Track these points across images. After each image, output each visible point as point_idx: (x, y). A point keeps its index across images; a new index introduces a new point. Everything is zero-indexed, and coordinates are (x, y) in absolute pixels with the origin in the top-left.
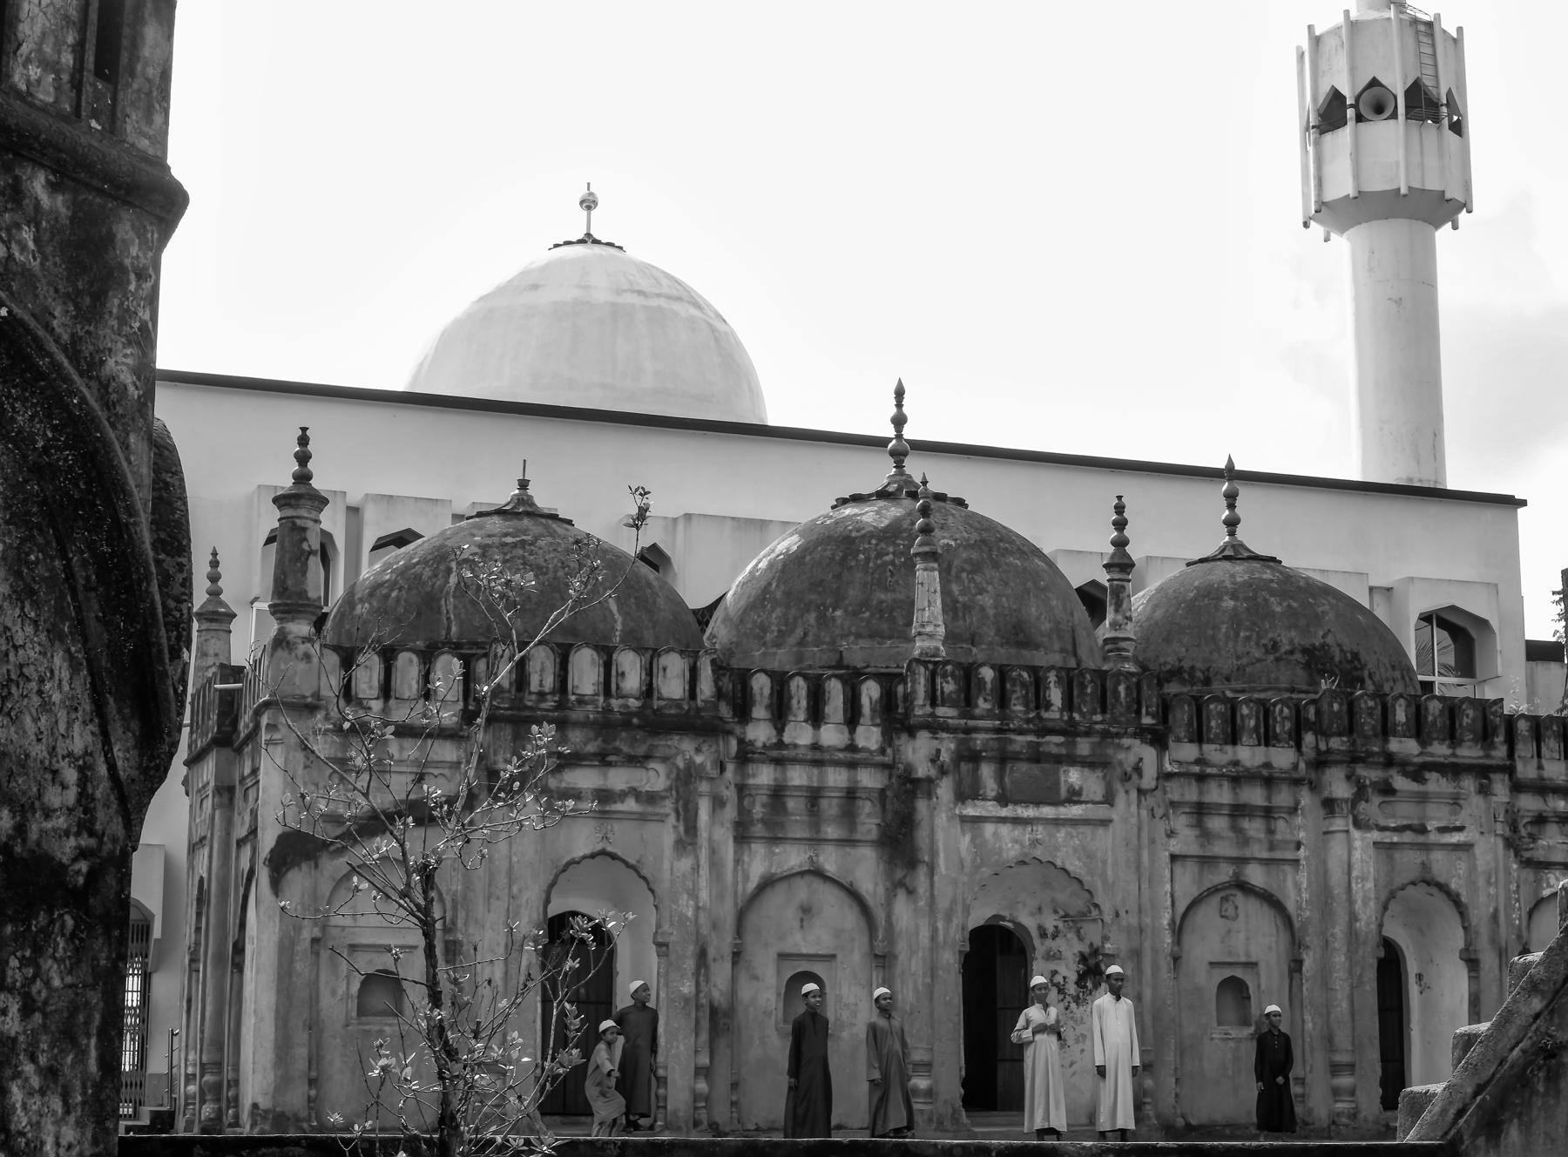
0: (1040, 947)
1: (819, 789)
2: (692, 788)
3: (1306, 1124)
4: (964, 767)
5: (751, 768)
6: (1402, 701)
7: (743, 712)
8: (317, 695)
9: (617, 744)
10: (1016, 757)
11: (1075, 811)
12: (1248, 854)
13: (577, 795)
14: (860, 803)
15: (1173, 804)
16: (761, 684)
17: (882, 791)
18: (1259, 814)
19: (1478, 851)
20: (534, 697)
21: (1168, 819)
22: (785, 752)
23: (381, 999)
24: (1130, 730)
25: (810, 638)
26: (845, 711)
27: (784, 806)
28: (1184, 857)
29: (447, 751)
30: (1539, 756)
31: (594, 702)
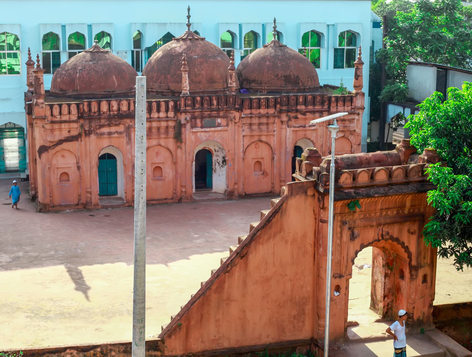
0: (215, 153)
3: (274, 193)
4: (193, 120)
6: (301, 97)
8: (45, 116)
9: (112, 122)
11: (219, 128)
12: (262, 134)
14: (169, 129)
15: (243, 124)
17: (174, 126)
19: (318, 131)
23: (65, 178)
25: (162, 82)
26: (165, 109)
27: (152, 131)
29: (75, 125)
30: (337, 106)
31: (107, 113)
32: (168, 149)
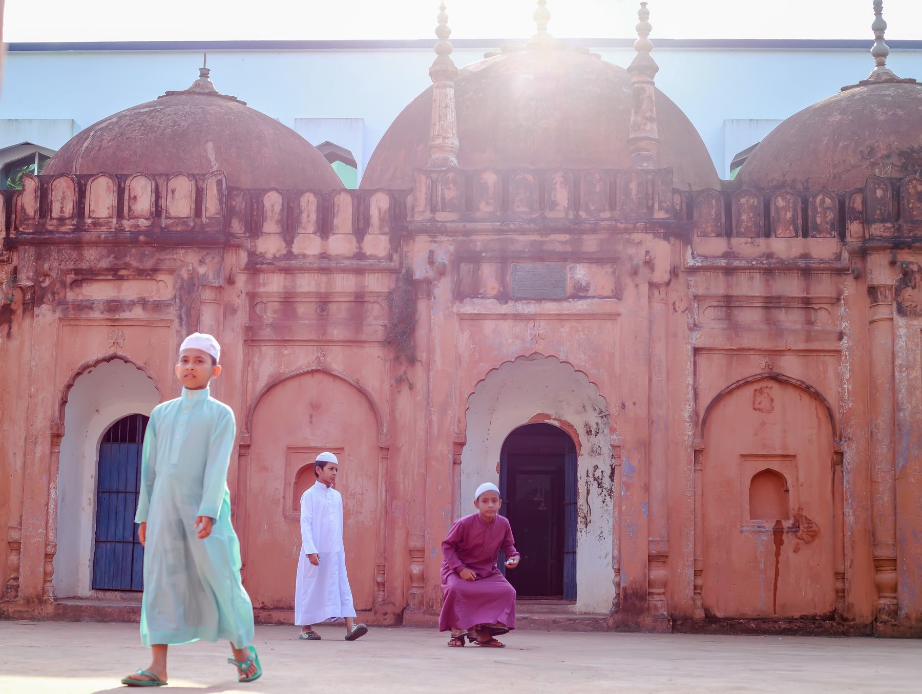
0: (585, 444)
1: (328, 295)
2: (194, 296)
3: (846, 620)
4: (465, 267)
5: (262, 278)
7: (254, 229)
9: (127, 259)
10: (519, 257)
11: (580, 306)
12: (781, 345)
13: (90, 306)
15: (696, 297)
16: (273, 202)
18: (796, 305)
20: (54, 222)
21: (692, 314)
22: (292, 262)
24: (638, 225)
28: (710, 349)
31: (107, 224)
32: (361, 391)
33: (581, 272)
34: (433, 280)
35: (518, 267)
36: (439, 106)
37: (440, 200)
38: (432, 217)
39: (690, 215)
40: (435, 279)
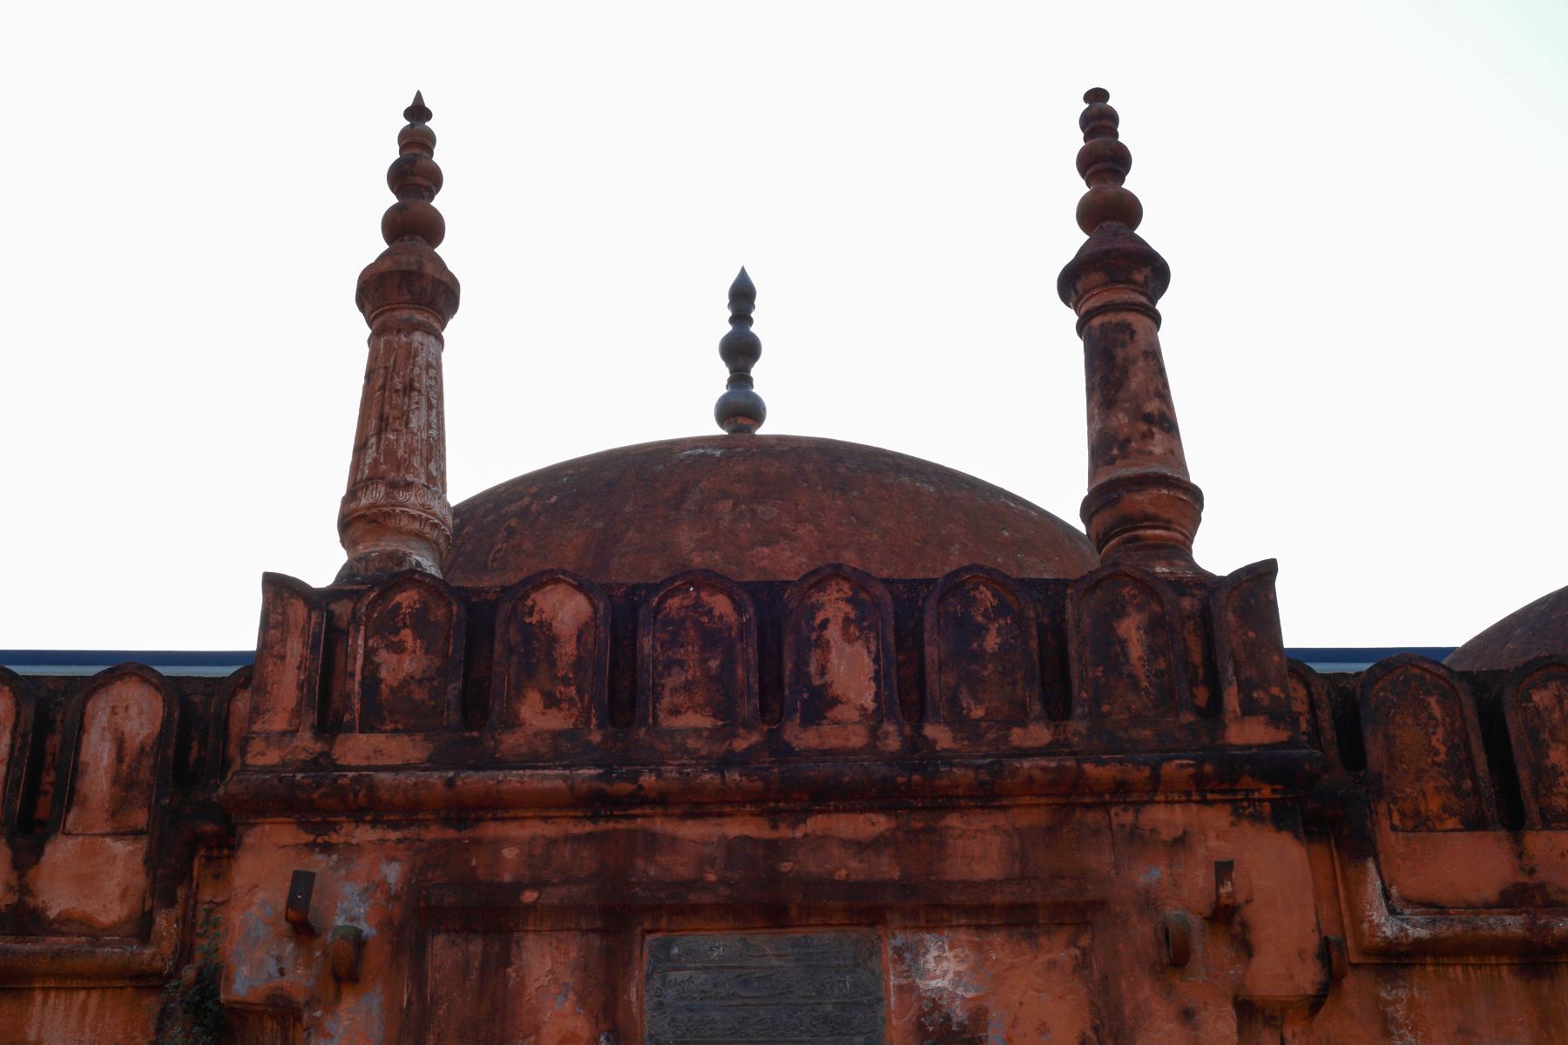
4: (443, 952)
24: (1169, 768)
33: (945, 964)
34: (307, 1004)
35: (675, 951)
36: (383, 388)
37: (357, 688)
38: (322, 754)
39: (1353, 753)
40: (313, 1001)
